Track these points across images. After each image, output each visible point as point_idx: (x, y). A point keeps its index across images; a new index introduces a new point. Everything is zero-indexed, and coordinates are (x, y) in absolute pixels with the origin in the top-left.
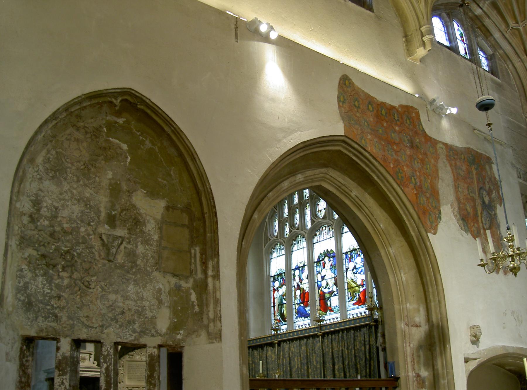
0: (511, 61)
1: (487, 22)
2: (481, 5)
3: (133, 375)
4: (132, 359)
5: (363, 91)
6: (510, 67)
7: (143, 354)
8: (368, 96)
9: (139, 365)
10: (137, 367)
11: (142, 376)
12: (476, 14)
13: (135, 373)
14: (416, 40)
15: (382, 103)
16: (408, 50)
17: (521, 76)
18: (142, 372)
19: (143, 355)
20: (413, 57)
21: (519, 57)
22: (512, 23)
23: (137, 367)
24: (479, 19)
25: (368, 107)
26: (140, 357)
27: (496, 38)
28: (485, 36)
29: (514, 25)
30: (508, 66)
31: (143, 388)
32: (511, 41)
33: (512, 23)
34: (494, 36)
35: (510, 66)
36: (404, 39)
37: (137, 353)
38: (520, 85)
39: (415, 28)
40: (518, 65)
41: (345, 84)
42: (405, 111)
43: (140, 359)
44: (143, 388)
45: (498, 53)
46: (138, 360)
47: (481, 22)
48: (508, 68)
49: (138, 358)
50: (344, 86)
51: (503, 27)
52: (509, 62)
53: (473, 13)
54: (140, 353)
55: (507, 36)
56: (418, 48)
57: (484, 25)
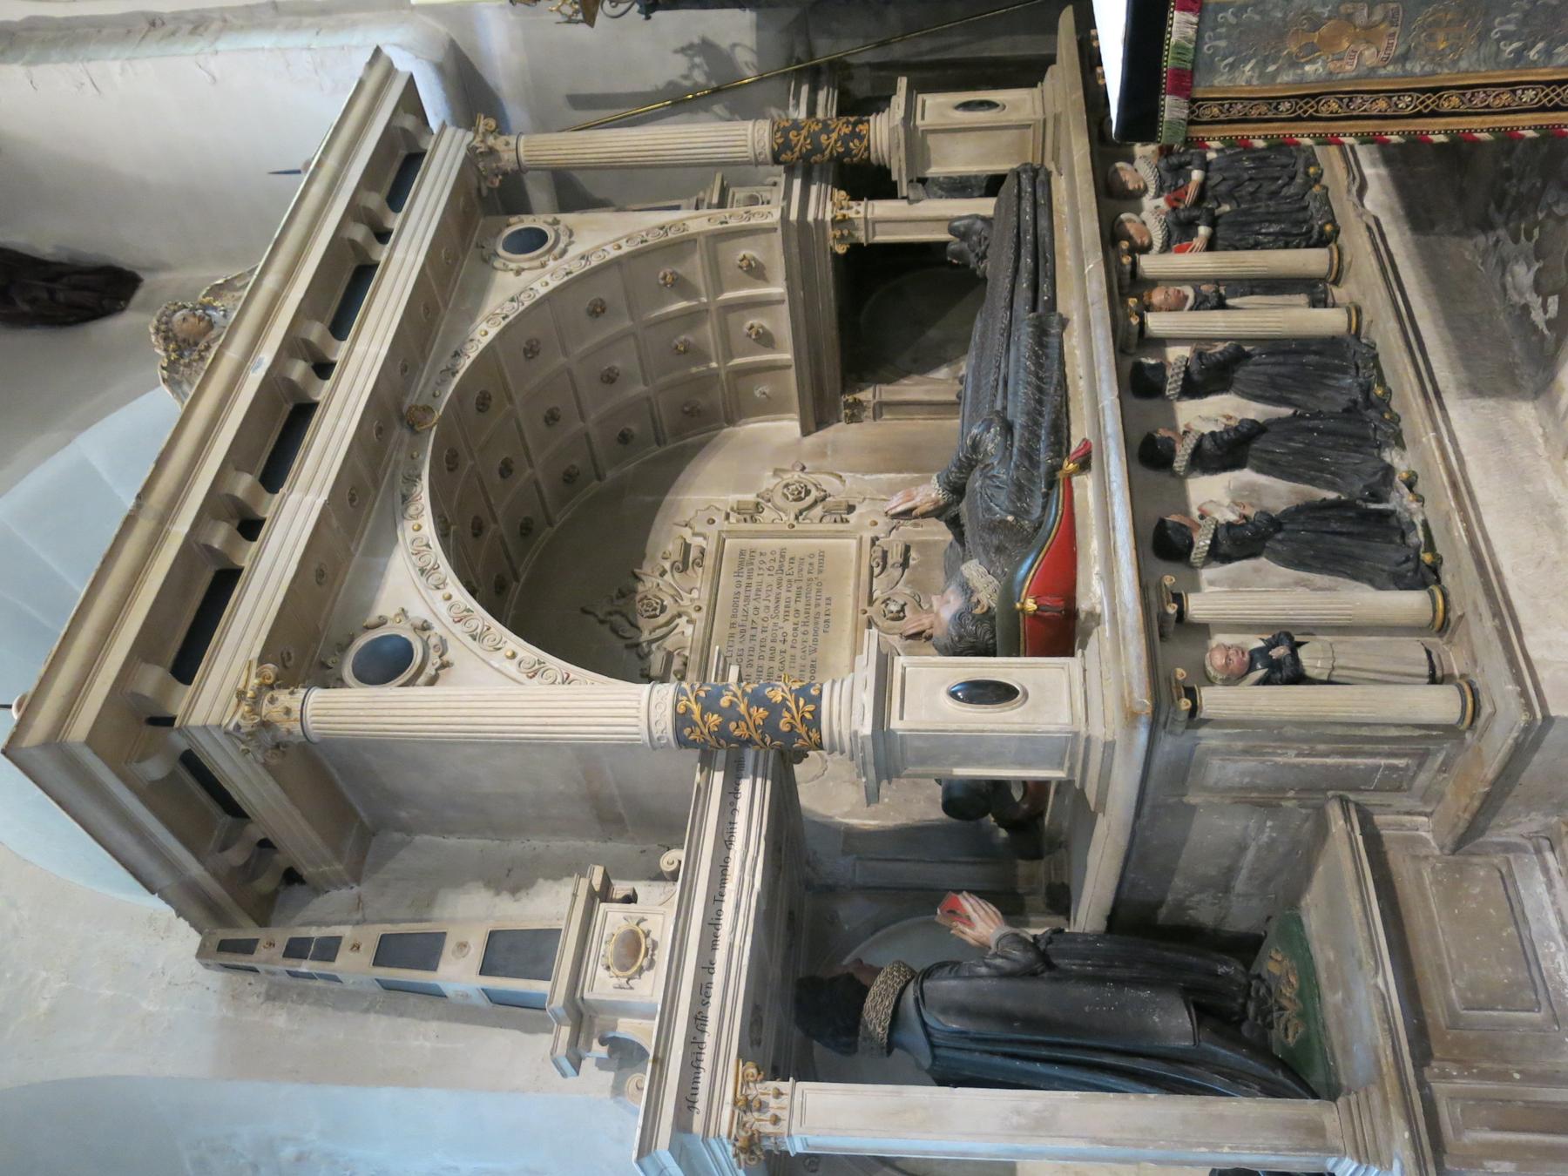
3: (793, 657)
4: (694, 659)
7: (668, 601)
9: (733, 625)
10: (743, 631)
11: (801, 606)
13: (779, 646)
18: (777, 607)
19: (676, 598)
23: (743, 631)
26: (684, 619)
31: (871, 602)
37: (659, 633)
43: (694, 615)
44: (871, 602)
46: (700, 625)
49: (689, 630)
54: (662, 619)
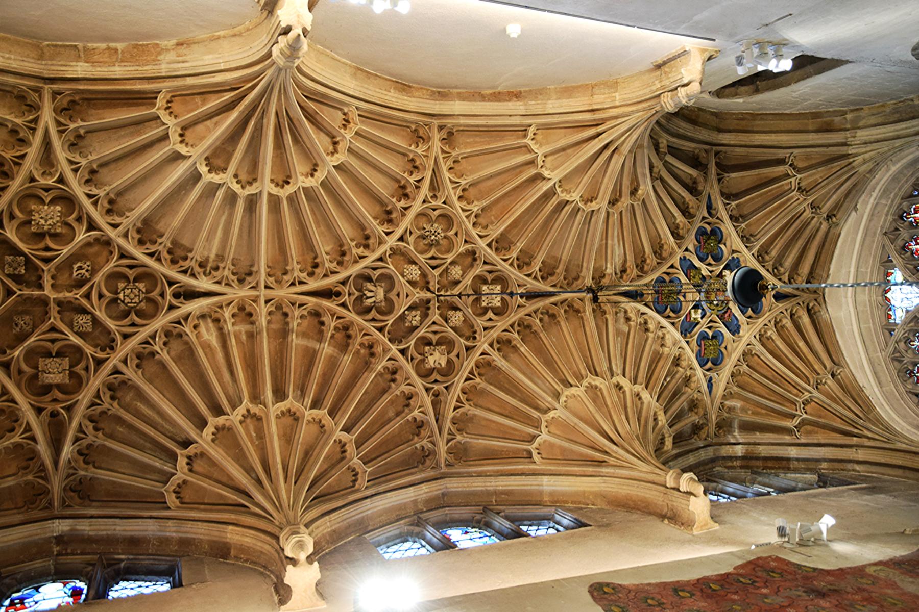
0: (850, 461)
1: (763, 451)
2: (732, 441)
5: (649, 584)
6: (858, 469)
8: (665, 585)
12: (740, 455)
14: (678, 502)
15: (698, 580)
16: (682, 524)
17: (883, 461)
20: (697, 524)
21: (851, 446)
22: (790, 424)
24: (752, 458)
25: (679, 595)
27: (796, 456)
28: (783, 468)
29: (794, 421)
30: (854, 470)
32: (816, 441)
33: (790, 424)
34: (792, 456)
35: (857, 467)
36: (666, 521)
38: (899, 472)
39: (662, 495)
40: (861, 455)
41: (605, 593)
42: (754, 569)
45: (824, 469)
47: (757, 458)
48: (858, 471)
50: (606, 596)
51: (787, 438)
52: (849, 466)
53: (737, 458)
55: (803, 441)
56: (688, 506)
57: (766, 459)
